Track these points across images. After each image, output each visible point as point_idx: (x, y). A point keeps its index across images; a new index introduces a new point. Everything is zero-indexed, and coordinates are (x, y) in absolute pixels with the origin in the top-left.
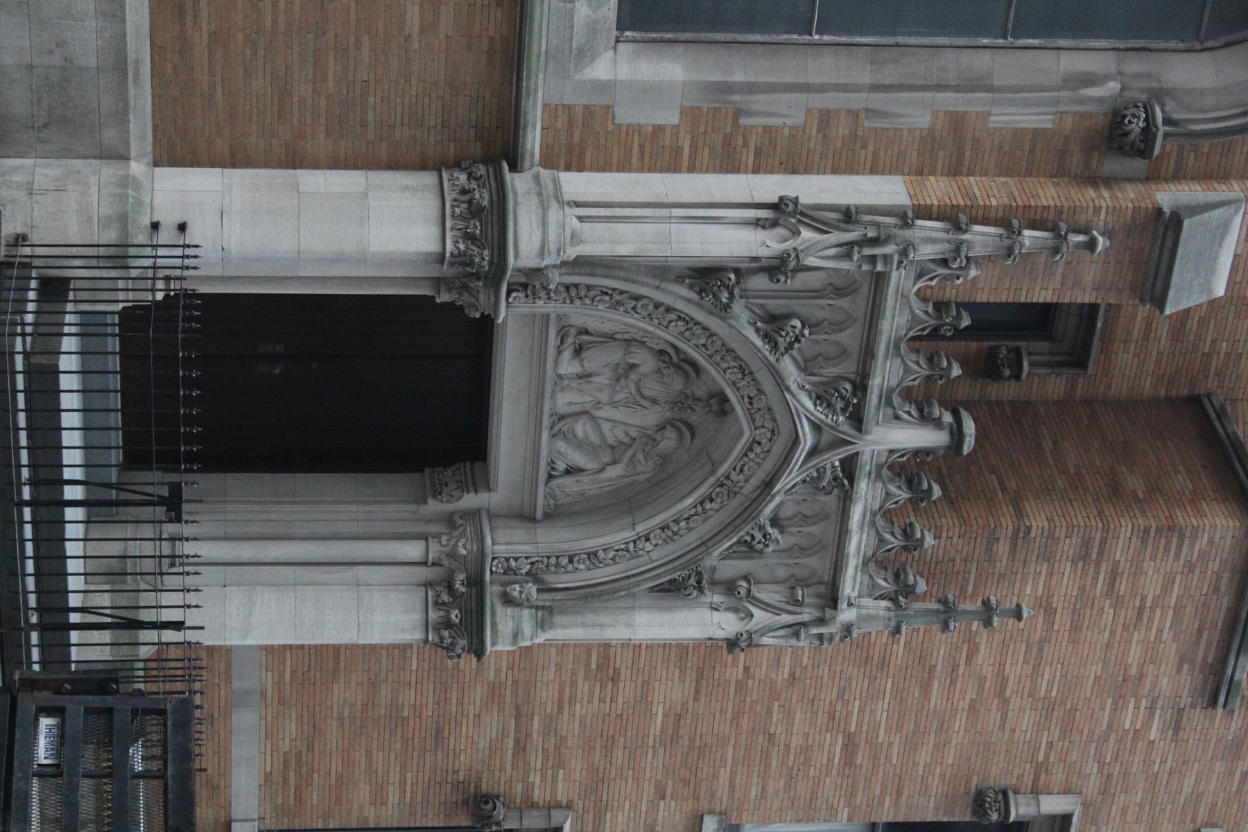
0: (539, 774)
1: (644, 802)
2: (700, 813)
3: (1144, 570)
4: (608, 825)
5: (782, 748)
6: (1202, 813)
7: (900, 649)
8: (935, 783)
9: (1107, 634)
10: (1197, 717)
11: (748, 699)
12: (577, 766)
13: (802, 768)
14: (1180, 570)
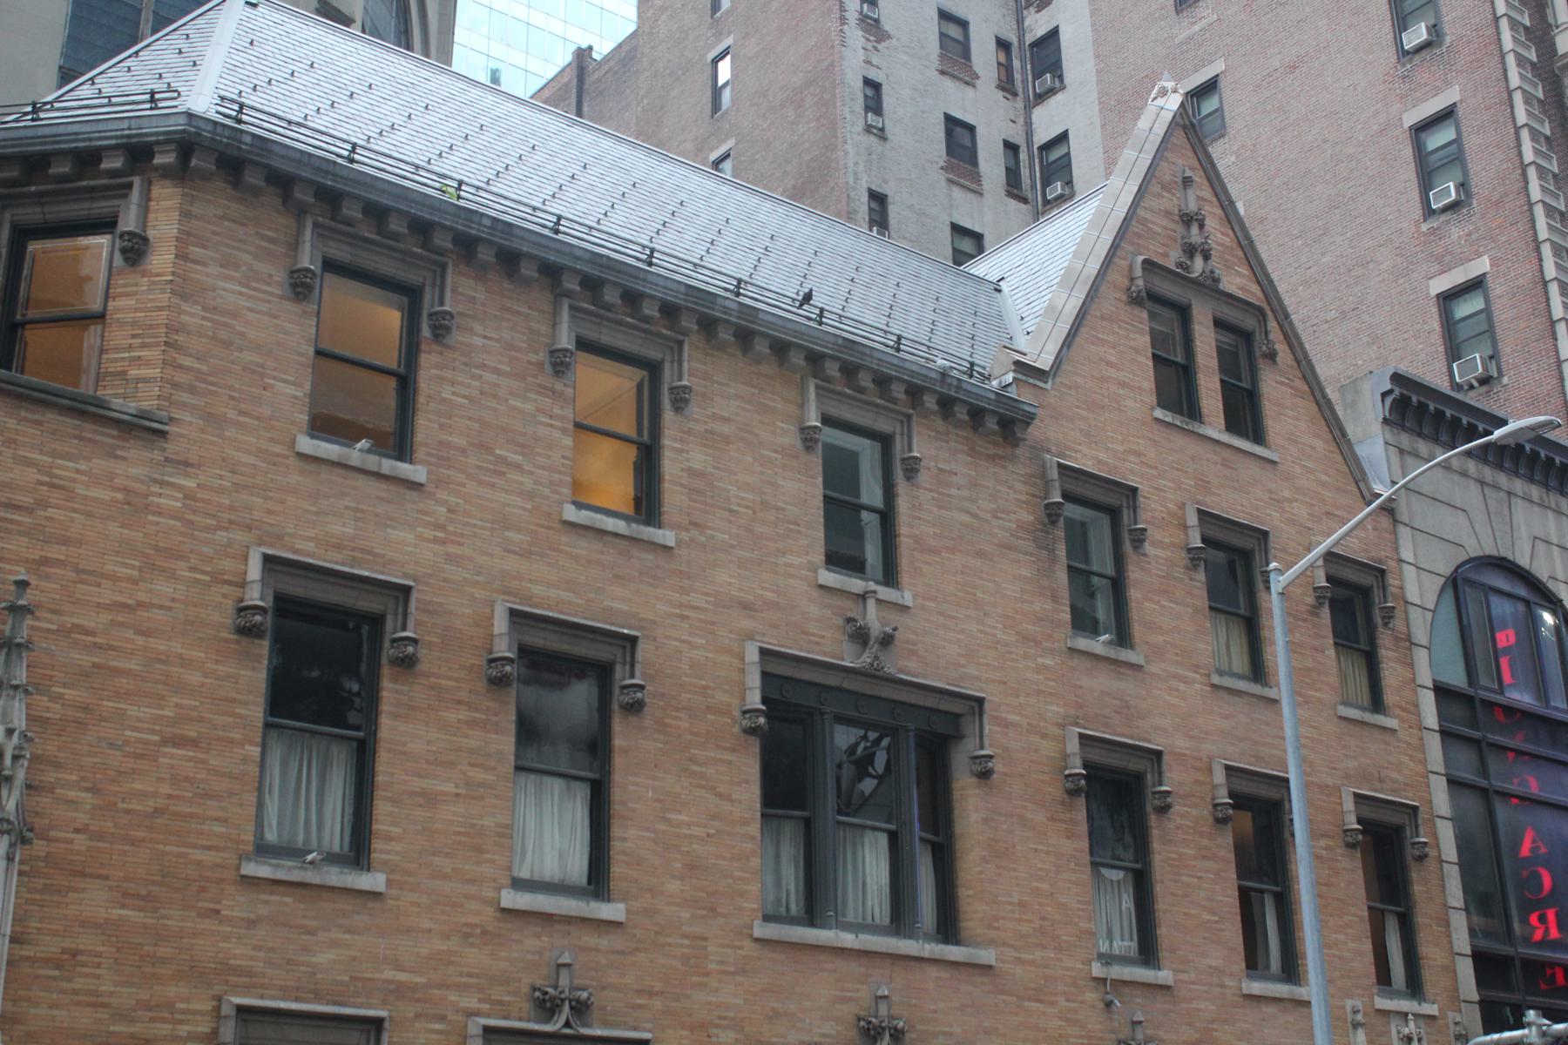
0: (179, 1027)
1: (220, 928)
2: (238, 878)
3: (8, 480)
4: (244, 963)
5: (171, 802)
6: (278, 449)
7: (70, 693)
8: (222, 669)
9: (76, 515)
10: (173, 448)
11: (113, 830)
12: (172, 991)
13: (195, 785)
14: (12, 451)
